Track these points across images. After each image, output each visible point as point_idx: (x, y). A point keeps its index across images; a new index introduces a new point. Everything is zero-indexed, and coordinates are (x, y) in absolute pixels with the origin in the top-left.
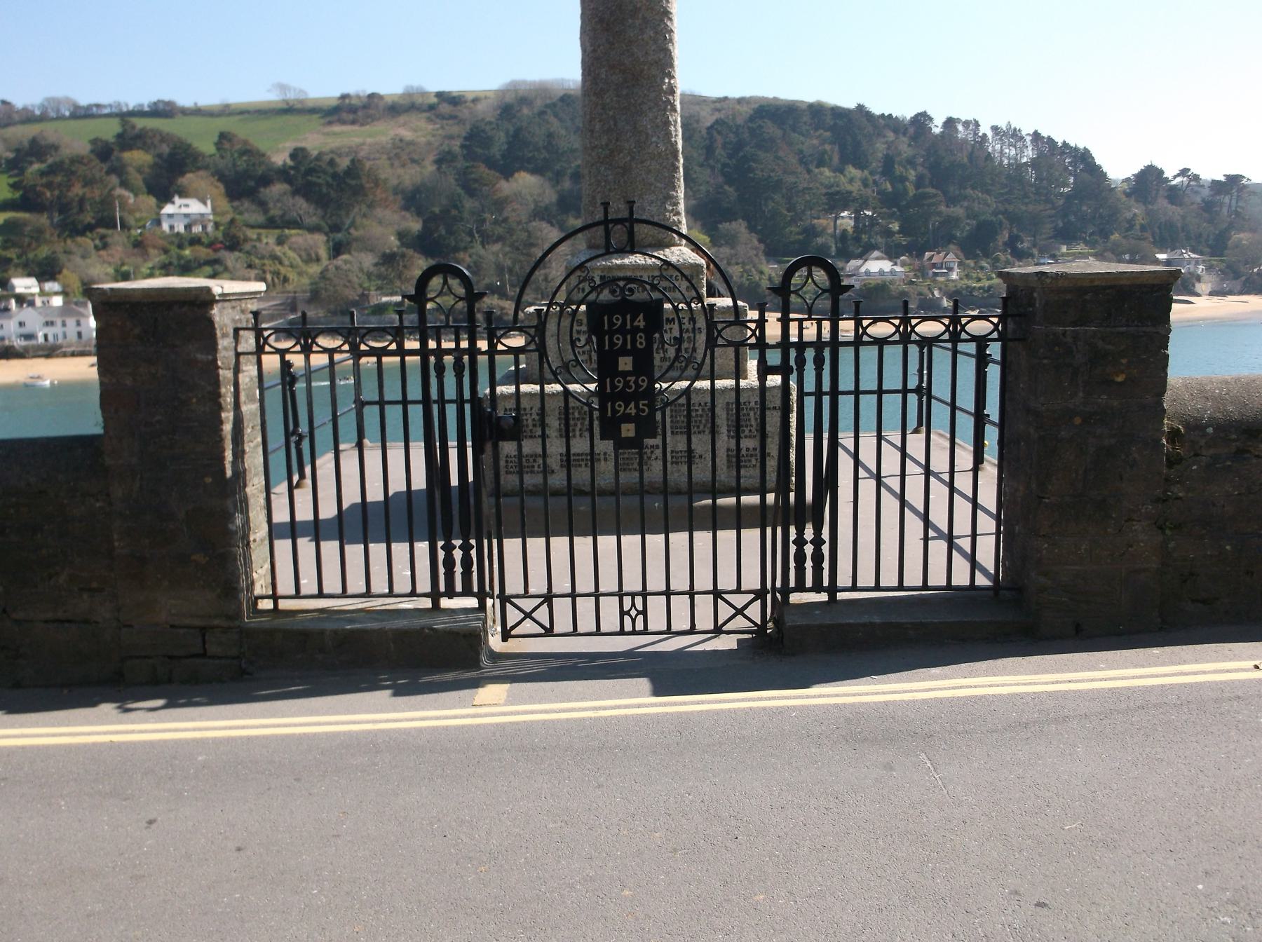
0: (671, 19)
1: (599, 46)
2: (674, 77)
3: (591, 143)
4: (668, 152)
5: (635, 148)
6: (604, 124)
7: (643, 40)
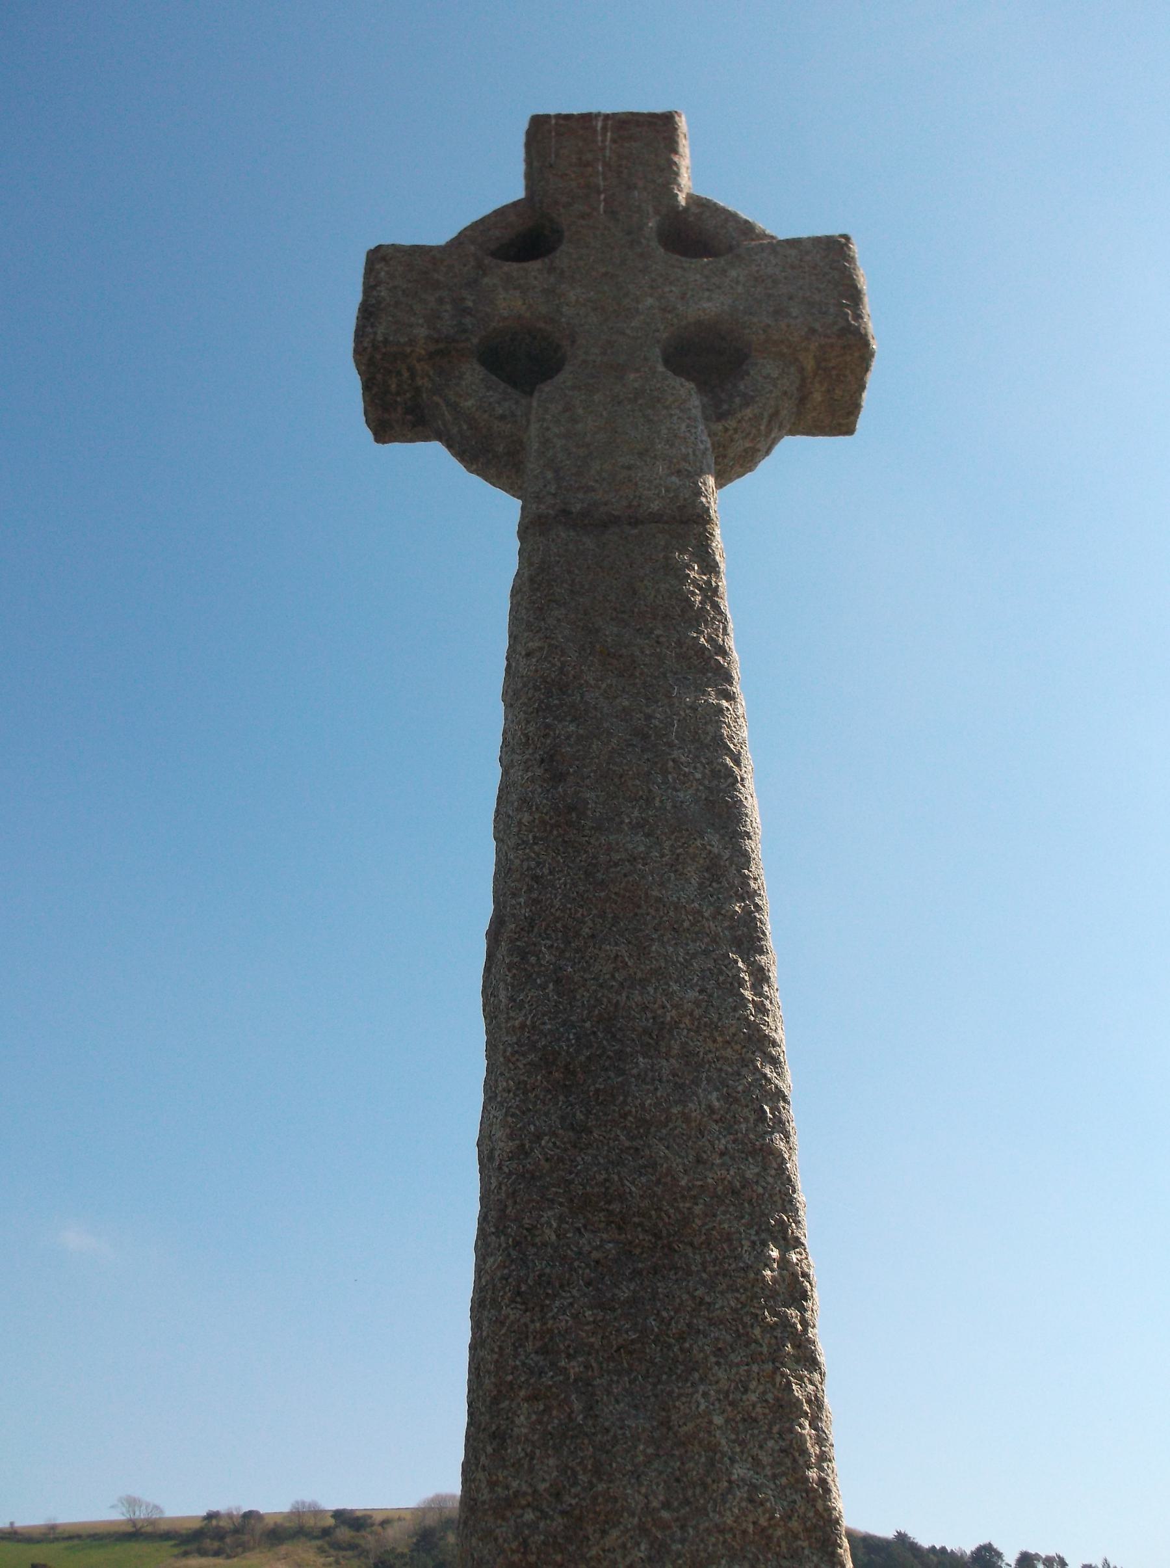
0: (775, 1062)
1: (538, 1137)
2: (797, 1243)
3: (492, 1485)
4: (794, 1524)
5: (666, 1505)
6: (548, 1409)
7: (687, 1119)
